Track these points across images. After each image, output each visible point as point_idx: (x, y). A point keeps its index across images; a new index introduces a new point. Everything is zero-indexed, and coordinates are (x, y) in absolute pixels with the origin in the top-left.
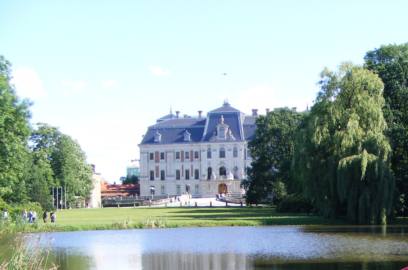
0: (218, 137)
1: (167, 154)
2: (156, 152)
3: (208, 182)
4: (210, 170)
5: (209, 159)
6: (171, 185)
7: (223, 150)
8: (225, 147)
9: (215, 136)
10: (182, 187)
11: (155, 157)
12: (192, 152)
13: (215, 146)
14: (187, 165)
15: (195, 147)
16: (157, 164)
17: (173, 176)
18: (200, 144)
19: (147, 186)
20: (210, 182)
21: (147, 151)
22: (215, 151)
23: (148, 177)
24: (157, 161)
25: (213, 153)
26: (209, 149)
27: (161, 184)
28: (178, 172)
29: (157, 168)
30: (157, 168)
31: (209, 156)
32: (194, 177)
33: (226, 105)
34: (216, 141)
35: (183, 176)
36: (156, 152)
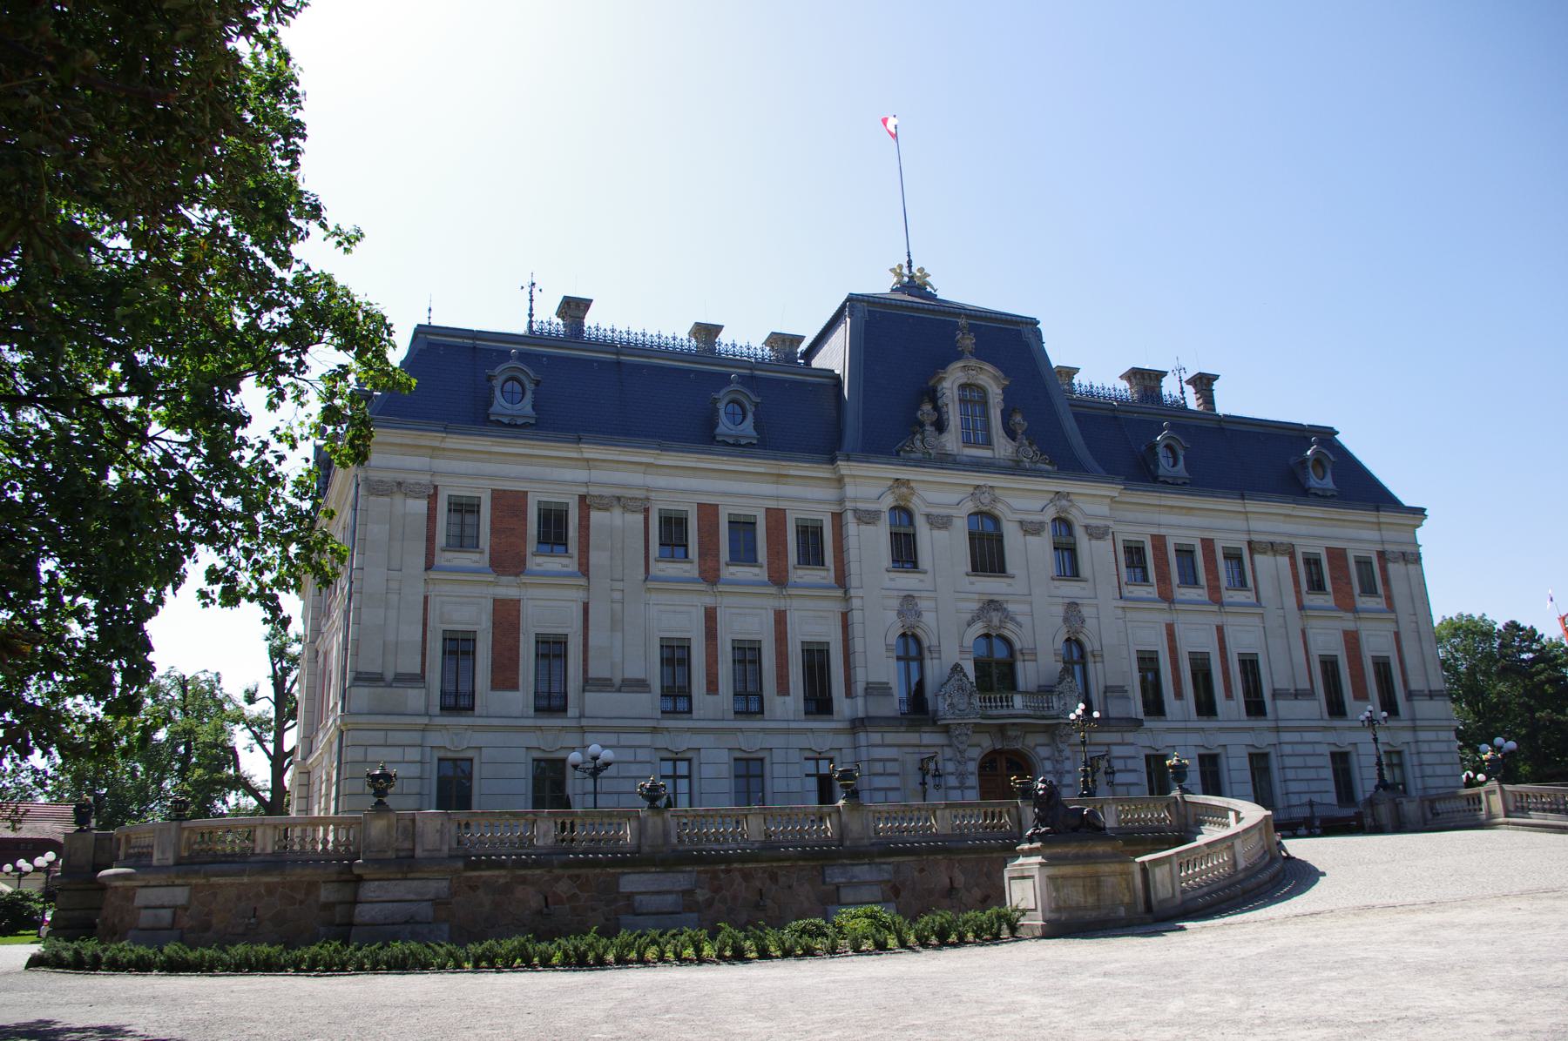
0: (951, 441)
1: (595, 516)
2: (497, 496)
3: (912, 738)
5: (907, 581)
7: (989, 527)
8: (1000, 510)
9: (929, 429)
10: (707, 771)
11: (493, 531)
13: (941, 494)
14: (747, 614)
15: (800, 490)
16: (507, 589)
17: (640, 685)
18: (844, 468)
19: (414, 754)
20: (928, 738)
21: (425, 479)
22: (940, 522)
23: (419, 679)
24: (507, 562)
27: (533, 740)
28: (675, 655)
29: (506, 617)
30: (506, 617)
31: (905, 552)
32: (794, 701)
33: (914, 285)
34: (945, 461)
35: (712, 687)
36: (497, 496)
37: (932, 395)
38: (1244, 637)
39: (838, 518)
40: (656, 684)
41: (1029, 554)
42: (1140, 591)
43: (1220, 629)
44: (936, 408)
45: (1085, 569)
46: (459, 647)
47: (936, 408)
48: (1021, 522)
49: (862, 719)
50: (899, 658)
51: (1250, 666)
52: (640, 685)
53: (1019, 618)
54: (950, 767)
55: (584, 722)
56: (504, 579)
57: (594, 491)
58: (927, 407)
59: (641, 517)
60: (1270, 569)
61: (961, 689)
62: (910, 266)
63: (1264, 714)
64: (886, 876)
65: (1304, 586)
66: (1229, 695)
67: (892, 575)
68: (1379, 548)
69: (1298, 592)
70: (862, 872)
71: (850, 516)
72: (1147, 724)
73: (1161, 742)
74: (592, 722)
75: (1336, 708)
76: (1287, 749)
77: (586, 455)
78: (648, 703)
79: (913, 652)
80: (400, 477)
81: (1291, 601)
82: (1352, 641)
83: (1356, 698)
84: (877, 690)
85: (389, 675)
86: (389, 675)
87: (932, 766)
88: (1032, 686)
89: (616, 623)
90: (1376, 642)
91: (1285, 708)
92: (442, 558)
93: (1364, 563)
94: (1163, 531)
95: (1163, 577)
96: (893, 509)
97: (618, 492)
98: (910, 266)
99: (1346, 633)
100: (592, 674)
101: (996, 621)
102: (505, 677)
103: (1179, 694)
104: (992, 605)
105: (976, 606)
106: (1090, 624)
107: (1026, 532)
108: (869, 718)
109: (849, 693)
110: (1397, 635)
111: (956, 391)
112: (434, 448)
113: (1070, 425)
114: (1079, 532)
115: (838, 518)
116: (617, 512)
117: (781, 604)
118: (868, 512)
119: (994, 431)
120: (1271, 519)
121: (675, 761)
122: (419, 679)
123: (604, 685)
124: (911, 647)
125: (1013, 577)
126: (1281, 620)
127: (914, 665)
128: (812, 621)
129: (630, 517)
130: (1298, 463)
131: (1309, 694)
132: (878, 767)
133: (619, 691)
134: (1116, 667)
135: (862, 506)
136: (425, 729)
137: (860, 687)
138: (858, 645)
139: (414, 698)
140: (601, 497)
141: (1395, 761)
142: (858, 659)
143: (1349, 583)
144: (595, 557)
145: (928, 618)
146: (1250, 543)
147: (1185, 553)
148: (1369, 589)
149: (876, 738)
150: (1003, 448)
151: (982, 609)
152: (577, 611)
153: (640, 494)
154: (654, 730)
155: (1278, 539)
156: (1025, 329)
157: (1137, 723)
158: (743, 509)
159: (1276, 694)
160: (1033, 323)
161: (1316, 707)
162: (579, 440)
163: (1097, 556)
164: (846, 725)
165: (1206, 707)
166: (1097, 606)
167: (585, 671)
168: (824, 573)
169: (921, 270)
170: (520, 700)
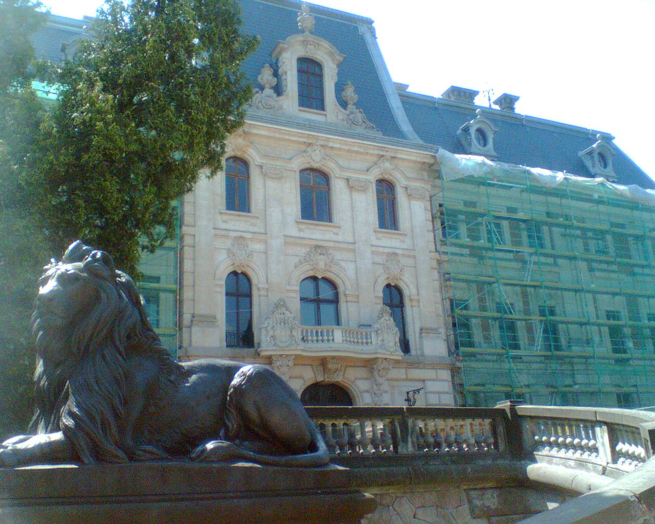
4: (239, 287)
5: (236, 223)
8: (330, 167)
9: (268, 91)
25: (258, 188)
41: (354, 208)
44: (276, 74)
47: (276, 74)
48: (348, 180)
53: (342, 264)
101: (322, 265)
105: (303, 251)
113: (395, 103)
125: (339, 227)
137: (187, 317)
156: (362, 29)
160: (369, 22)
166: (415, 257)
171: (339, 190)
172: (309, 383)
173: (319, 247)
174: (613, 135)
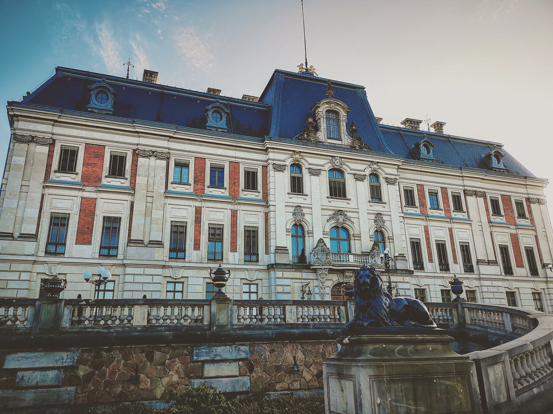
0: (322, 136)
1: (141, 160)
3: (298, 275)
5: (297, 199)
6: (148, 279)
11: (84, 164)
12: (234, 166)
17: (159, 244)
19: (24, 276)
22: (315, 173)
23: (34, 237)
25: (308, 180)
26: (297, 166)
28: (178, 231)
31: (297, 186)
34: (318, 143)
37: (314, 116)
38: (462, 234)
39: (265, 168)
40: (167, 244)
41: (357, 191)
42: (411, 210)
43: (450, 230)
44: (315, 120)
45: (385, 198)
46: (59, 222)
48: (354, 174)
49: (272, 265)
50: (292, 236)
51: (465, 249)
52: (159, 244)
53: (352, 219)
54: (317, 290)
55: (125, 262)
56: (88, 188)
57: (140, 147)
58: (310, 120)
59: (165, 162)
60: (474, 205)
61: (323, 251)
62: (306, 65)
63: (473, 272)
64: (243, 355)
65: (491, 212)
66: (455, 262)
67: (291, 196)
68: (527, 196)
69: (488, 215)
70: (223, 351)
71: (271, 167)
72: (415, 274)
73: (423, 283)
74: (129, 262)
75: (508, 271)
76: (485, 289)
77: (137, 130)
78: (162, 254)
79: (300, 233)
80: (34, 134)
81: (485, 219)
82: (515, 239)
83: (517, 266)
84: (281, 250)
85: (16, 235)
86: (16, 235)
87: (307, 289)
88: (359, 252)
89: (148, 213)
90: (526, 240)
91: (485, 269)
92: (54, 176)
93: (519, 204)
94: (423, 183)
95: (423, 205)
96: (292, 165)
97: (154, 149)
98: (306, 65)
99: (512, 235)
100: (132, 238)
101: (341, 220)
102: (84, 237)
103: (431, 260)
104: (340, 212)
106: (387, 224)
107: (357, 179)
108: (276, 264)
109: (267, 252)
110: (536, 237)
111: (324, 113)
112: (55, 121)
114: (382, 181)
115: (265, 168)
116: (153, 159)
117: (236, 207)
118: (280, 165)
119: (342, 132)
120: (474, 181)
121: (175, 283)
122: (34, 237)
123: (139, 242)
124: (299, 230)
126: (480, 228)
127: (300, 240)
128: (251, 217)
129: (158, 161)
130: (486, 158)
131: (495, 263)
132: (280, 289)
133: (147, 246)
134: (399, 245)
135: (275, 162)
136: (35, 262)
137: (272, 249)
138: (272, 228)
139: (29, 247)
140: (144, 151)
141: (537, 297)
142: (272, 235)
143: (512, 212)
144: (139, 180)
145: (307, 217)
146: (464, 191)
147: (434, 194)
148: (522, 215)
149: (279, 274)
150: (346, 140)
151: (334, 214)
152: (128, 205)
153: (166, 151)
154: (164, 267)
155: (478, 190)
157: (410, 273)
158: (218, 162)
159: (478, 262)
161: (497, 270)
162: (134, 122)
163: (392, 194)
164: (265, 268)
165: (444, 267)
166: (390, 215)
167: (129, 235)
168: (257, 194)
169: (311, 67)
170: (90, 251)
171: (349, 181)
172: (335, 283)
173: (340, 211)
174: (503, 144)
